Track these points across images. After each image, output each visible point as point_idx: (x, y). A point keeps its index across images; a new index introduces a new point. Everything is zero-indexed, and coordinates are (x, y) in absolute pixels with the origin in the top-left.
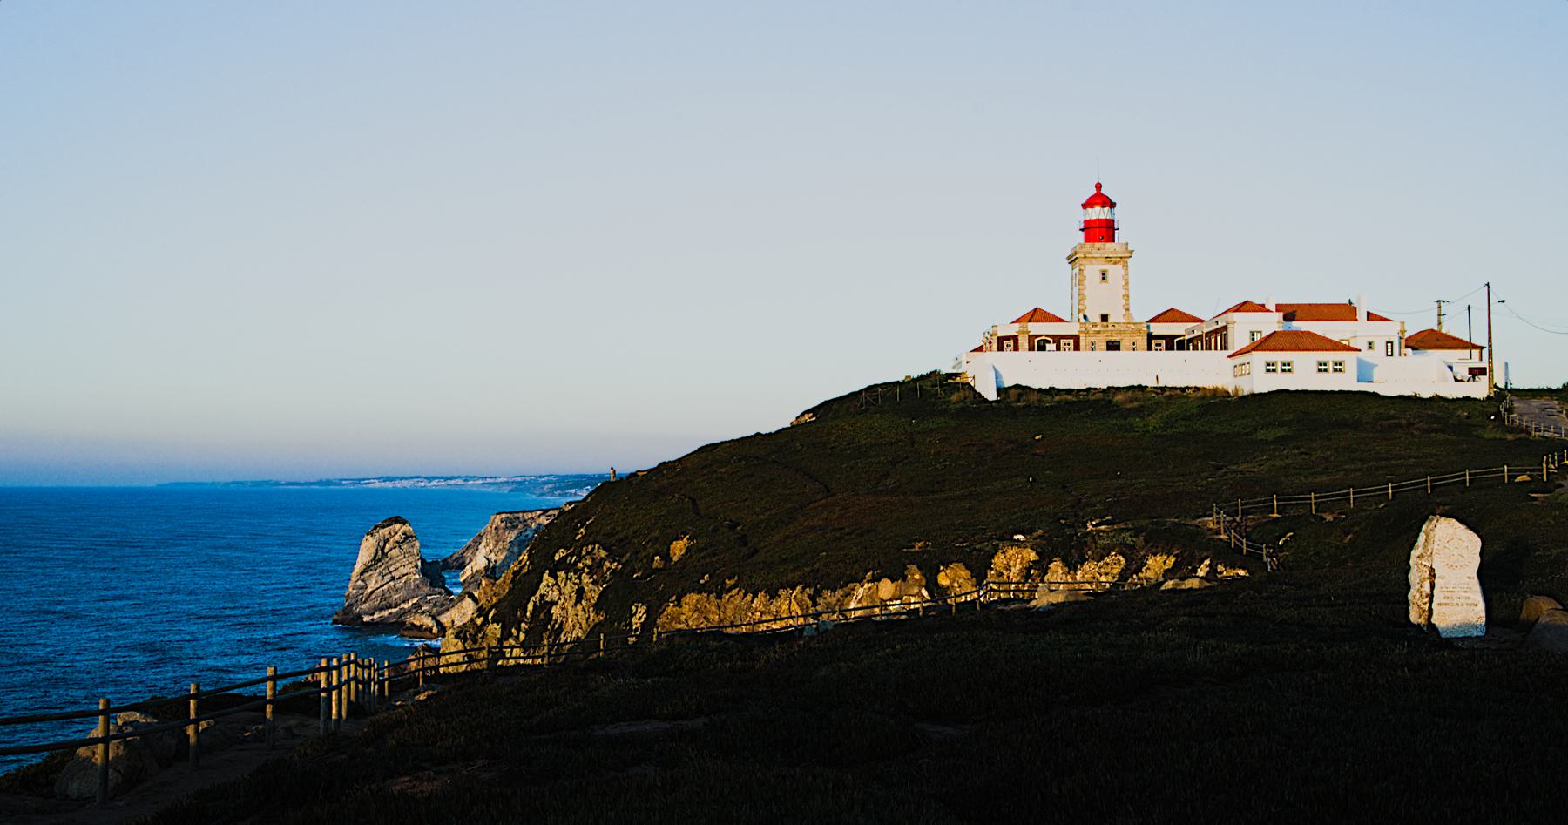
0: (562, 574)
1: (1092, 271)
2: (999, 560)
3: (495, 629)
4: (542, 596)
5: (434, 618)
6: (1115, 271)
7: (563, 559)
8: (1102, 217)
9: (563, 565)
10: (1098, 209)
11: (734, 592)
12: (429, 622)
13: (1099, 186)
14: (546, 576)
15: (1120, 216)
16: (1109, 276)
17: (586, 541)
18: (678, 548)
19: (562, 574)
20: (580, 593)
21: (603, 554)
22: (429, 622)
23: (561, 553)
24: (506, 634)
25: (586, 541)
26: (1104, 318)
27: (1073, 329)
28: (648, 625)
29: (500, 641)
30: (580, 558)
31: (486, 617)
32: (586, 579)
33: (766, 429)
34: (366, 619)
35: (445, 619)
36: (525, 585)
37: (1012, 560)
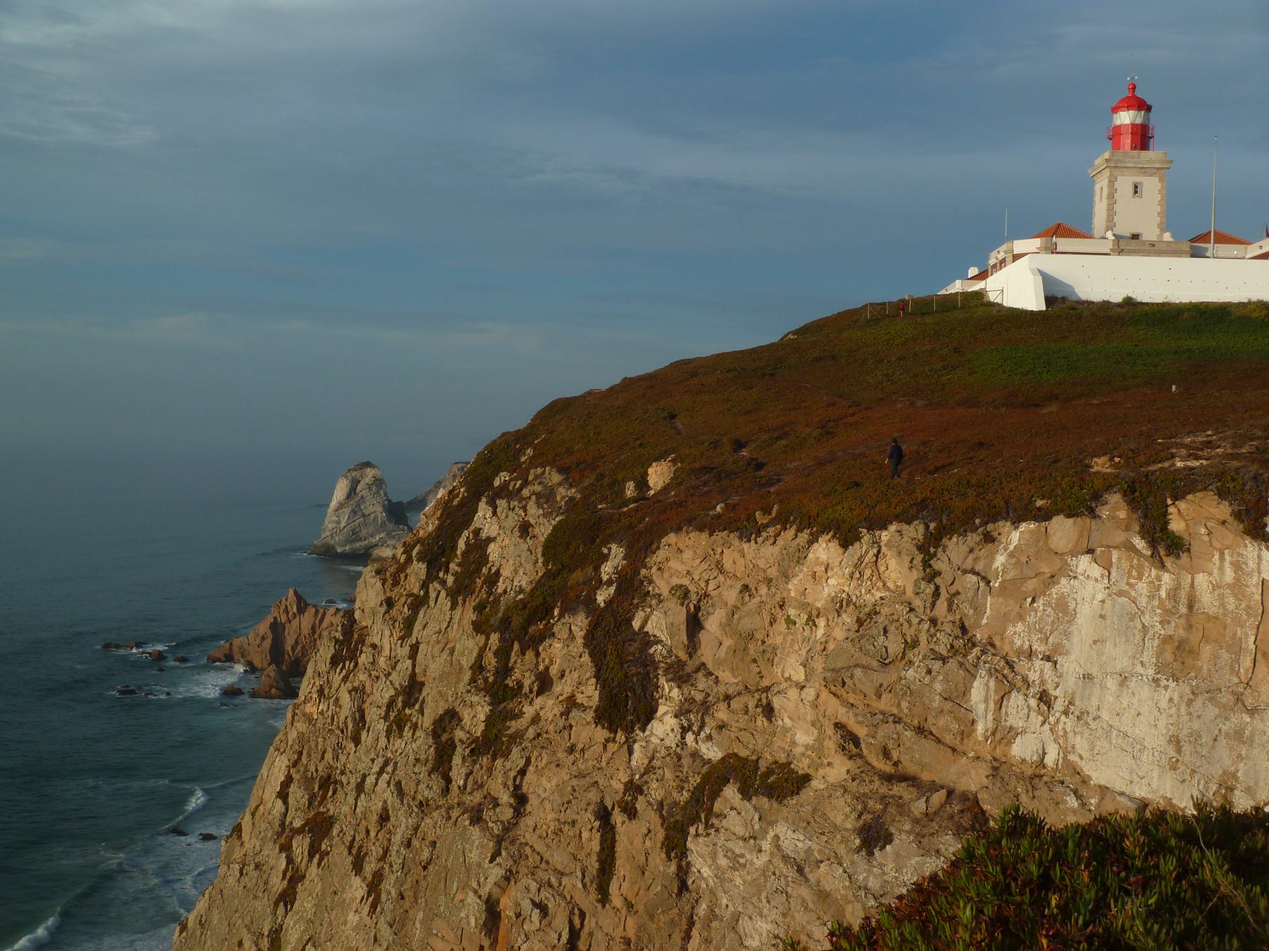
0: (501, 504)
1: (1125, 184)
3: (419, 569)
7: (505, 486)
8: (1139, 121)
10: (1132, 113)
11: (771, 530)
13: (1134, 88)
15: (1155, 119)
17: (533, 462)
18: (658, 475)
19: (501, 504)
21: (556, 478)
23: (503, 476)
24: (431, 576)
25: (533, 462)
29: (425, 585)
30: (526, 483)
32: (532, 509)
34: (339, 550)
36: (457, 516)
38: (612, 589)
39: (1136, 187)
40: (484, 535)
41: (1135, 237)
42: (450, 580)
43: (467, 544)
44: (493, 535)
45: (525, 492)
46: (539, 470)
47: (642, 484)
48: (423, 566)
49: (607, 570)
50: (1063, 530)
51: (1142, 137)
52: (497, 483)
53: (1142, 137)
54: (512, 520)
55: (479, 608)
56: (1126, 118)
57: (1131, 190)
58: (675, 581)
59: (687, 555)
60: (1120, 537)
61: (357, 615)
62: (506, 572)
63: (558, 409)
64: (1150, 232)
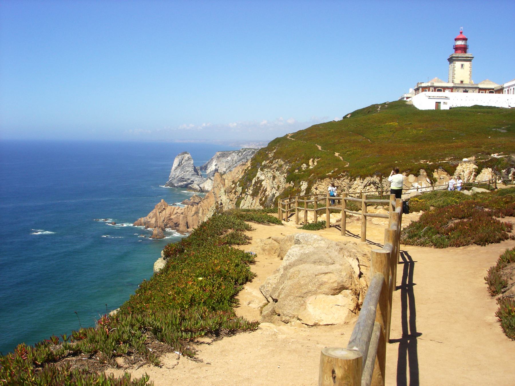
1: (458, 64)
2: (459, 168)
3: (239, 189)
4: (258, 178)
5: (198, 185)
6: (467, 64)
9: (265, 166)
11: (345, 178)
12: (197, 187)
13: (461, 33)
14: (259, 170)
15: (468, 43)
16: (465, 67)
17: (274, 158)
20: (274, 177)
21: (283, 163)
22: (197, 187)
24: (243, 192)
25: (274, 158)
26: (462, 82)
27: (451, 85)
28: (308, 190)
29: (241, 194)
31: (236, 184)
33: (336, 120)
34: (176, 185)
35: (201, 186)
37: (466, 168)
38: (304, 192)
39: (462, 65)
40: (260, 179)
41: (462, 82)
42: (251, 192)
43: (255, 182)
44: (263, 179)
45: (273, 167)
46: (276, 160)
47: (308, 165)
48: (241, 188)
49: (302, 187)
50: (412, 177)
51: (464, 49)
52: (263, 164)
53: (464, 49)
54: (270, 175)
55: (261, 200)
56: (460, 43)
57: (460, 66)
58: (321, 190)
59: (323, 184)
60: (424, 179)
61: (219, 203)
62: (268, 189)
63: (277, 141)
64: (467, 82)
